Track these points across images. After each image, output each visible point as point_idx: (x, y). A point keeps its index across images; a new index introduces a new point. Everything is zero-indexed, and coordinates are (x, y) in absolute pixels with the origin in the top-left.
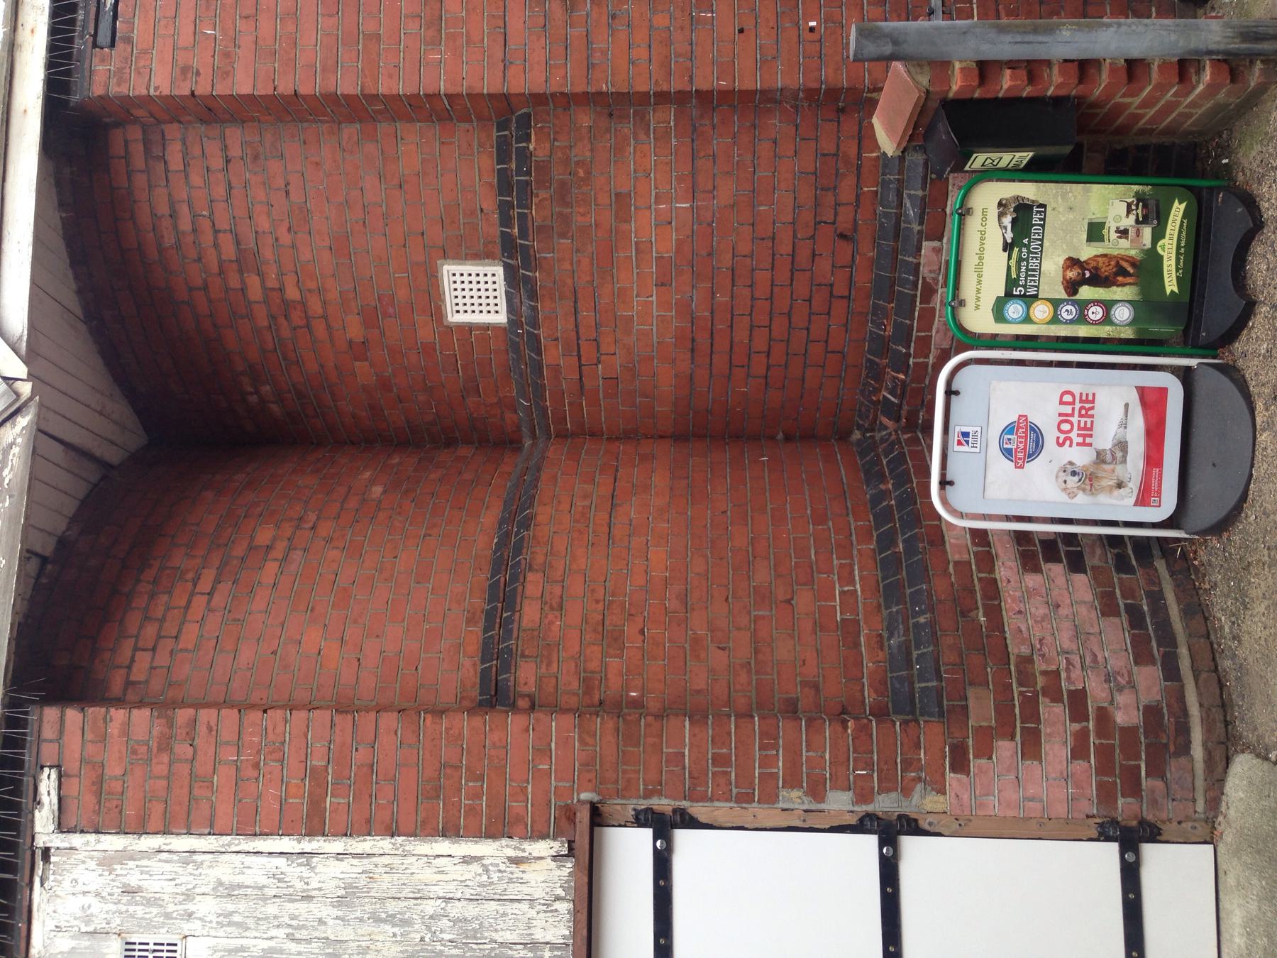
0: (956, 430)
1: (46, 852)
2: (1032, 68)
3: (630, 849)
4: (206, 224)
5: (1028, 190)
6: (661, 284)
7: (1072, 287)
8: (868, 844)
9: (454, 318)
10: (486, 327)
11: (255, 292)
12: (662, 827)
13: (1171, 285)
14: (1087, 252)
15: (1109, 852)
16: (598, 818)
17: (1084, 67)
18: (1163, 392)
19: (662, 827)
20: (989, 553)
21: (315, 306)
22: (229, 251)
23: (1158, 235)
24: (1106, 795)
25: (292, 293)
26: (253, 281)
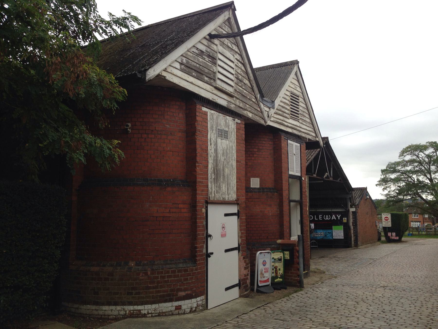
0: (265, 254)
1: (234, 120)
2: (298, 257)
3: (234, 209)
4: (263, 145)
5: (282, 260)
6: (261, 211)
7: (275, 268)
8: (237, 246)
9: (251, 179)
10: (250, 184)
11: (255, 150)
12: (238, 214)
13: (276, 281)
14: (278, 269)
15: (237, 282)
16: (238, 204)
17: (298, 263)
18: (268, 281)
19: (238, 214)
20: (351, 247)
21: (253, 158)
22: (261, 148)
23: (280, 278)
24: (242, 279)
25: (255, 155)
26: (256, 150)
